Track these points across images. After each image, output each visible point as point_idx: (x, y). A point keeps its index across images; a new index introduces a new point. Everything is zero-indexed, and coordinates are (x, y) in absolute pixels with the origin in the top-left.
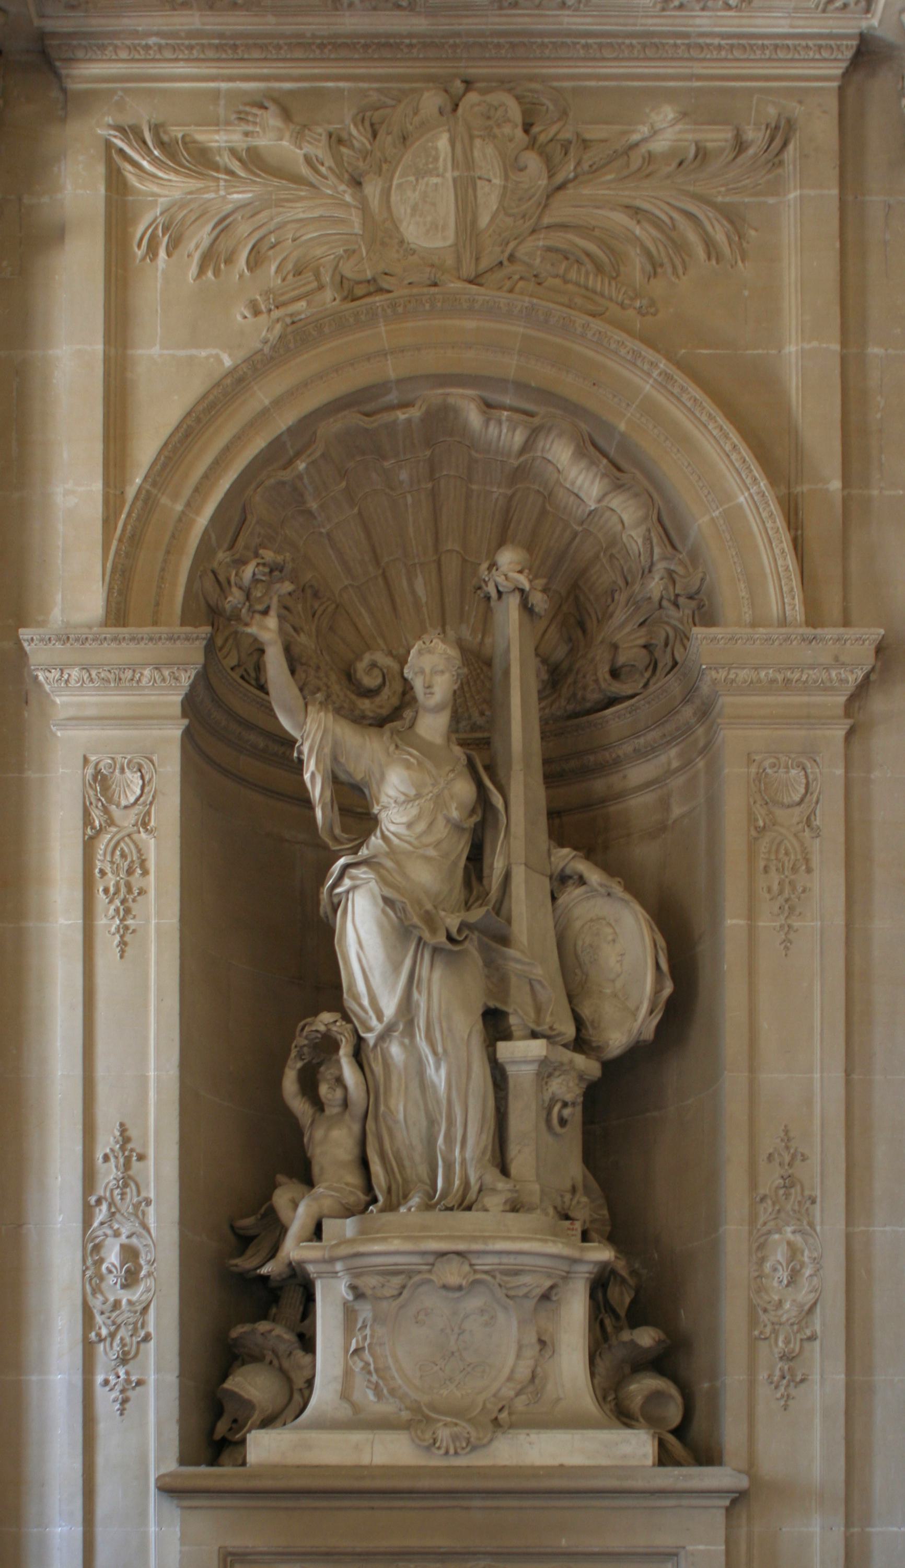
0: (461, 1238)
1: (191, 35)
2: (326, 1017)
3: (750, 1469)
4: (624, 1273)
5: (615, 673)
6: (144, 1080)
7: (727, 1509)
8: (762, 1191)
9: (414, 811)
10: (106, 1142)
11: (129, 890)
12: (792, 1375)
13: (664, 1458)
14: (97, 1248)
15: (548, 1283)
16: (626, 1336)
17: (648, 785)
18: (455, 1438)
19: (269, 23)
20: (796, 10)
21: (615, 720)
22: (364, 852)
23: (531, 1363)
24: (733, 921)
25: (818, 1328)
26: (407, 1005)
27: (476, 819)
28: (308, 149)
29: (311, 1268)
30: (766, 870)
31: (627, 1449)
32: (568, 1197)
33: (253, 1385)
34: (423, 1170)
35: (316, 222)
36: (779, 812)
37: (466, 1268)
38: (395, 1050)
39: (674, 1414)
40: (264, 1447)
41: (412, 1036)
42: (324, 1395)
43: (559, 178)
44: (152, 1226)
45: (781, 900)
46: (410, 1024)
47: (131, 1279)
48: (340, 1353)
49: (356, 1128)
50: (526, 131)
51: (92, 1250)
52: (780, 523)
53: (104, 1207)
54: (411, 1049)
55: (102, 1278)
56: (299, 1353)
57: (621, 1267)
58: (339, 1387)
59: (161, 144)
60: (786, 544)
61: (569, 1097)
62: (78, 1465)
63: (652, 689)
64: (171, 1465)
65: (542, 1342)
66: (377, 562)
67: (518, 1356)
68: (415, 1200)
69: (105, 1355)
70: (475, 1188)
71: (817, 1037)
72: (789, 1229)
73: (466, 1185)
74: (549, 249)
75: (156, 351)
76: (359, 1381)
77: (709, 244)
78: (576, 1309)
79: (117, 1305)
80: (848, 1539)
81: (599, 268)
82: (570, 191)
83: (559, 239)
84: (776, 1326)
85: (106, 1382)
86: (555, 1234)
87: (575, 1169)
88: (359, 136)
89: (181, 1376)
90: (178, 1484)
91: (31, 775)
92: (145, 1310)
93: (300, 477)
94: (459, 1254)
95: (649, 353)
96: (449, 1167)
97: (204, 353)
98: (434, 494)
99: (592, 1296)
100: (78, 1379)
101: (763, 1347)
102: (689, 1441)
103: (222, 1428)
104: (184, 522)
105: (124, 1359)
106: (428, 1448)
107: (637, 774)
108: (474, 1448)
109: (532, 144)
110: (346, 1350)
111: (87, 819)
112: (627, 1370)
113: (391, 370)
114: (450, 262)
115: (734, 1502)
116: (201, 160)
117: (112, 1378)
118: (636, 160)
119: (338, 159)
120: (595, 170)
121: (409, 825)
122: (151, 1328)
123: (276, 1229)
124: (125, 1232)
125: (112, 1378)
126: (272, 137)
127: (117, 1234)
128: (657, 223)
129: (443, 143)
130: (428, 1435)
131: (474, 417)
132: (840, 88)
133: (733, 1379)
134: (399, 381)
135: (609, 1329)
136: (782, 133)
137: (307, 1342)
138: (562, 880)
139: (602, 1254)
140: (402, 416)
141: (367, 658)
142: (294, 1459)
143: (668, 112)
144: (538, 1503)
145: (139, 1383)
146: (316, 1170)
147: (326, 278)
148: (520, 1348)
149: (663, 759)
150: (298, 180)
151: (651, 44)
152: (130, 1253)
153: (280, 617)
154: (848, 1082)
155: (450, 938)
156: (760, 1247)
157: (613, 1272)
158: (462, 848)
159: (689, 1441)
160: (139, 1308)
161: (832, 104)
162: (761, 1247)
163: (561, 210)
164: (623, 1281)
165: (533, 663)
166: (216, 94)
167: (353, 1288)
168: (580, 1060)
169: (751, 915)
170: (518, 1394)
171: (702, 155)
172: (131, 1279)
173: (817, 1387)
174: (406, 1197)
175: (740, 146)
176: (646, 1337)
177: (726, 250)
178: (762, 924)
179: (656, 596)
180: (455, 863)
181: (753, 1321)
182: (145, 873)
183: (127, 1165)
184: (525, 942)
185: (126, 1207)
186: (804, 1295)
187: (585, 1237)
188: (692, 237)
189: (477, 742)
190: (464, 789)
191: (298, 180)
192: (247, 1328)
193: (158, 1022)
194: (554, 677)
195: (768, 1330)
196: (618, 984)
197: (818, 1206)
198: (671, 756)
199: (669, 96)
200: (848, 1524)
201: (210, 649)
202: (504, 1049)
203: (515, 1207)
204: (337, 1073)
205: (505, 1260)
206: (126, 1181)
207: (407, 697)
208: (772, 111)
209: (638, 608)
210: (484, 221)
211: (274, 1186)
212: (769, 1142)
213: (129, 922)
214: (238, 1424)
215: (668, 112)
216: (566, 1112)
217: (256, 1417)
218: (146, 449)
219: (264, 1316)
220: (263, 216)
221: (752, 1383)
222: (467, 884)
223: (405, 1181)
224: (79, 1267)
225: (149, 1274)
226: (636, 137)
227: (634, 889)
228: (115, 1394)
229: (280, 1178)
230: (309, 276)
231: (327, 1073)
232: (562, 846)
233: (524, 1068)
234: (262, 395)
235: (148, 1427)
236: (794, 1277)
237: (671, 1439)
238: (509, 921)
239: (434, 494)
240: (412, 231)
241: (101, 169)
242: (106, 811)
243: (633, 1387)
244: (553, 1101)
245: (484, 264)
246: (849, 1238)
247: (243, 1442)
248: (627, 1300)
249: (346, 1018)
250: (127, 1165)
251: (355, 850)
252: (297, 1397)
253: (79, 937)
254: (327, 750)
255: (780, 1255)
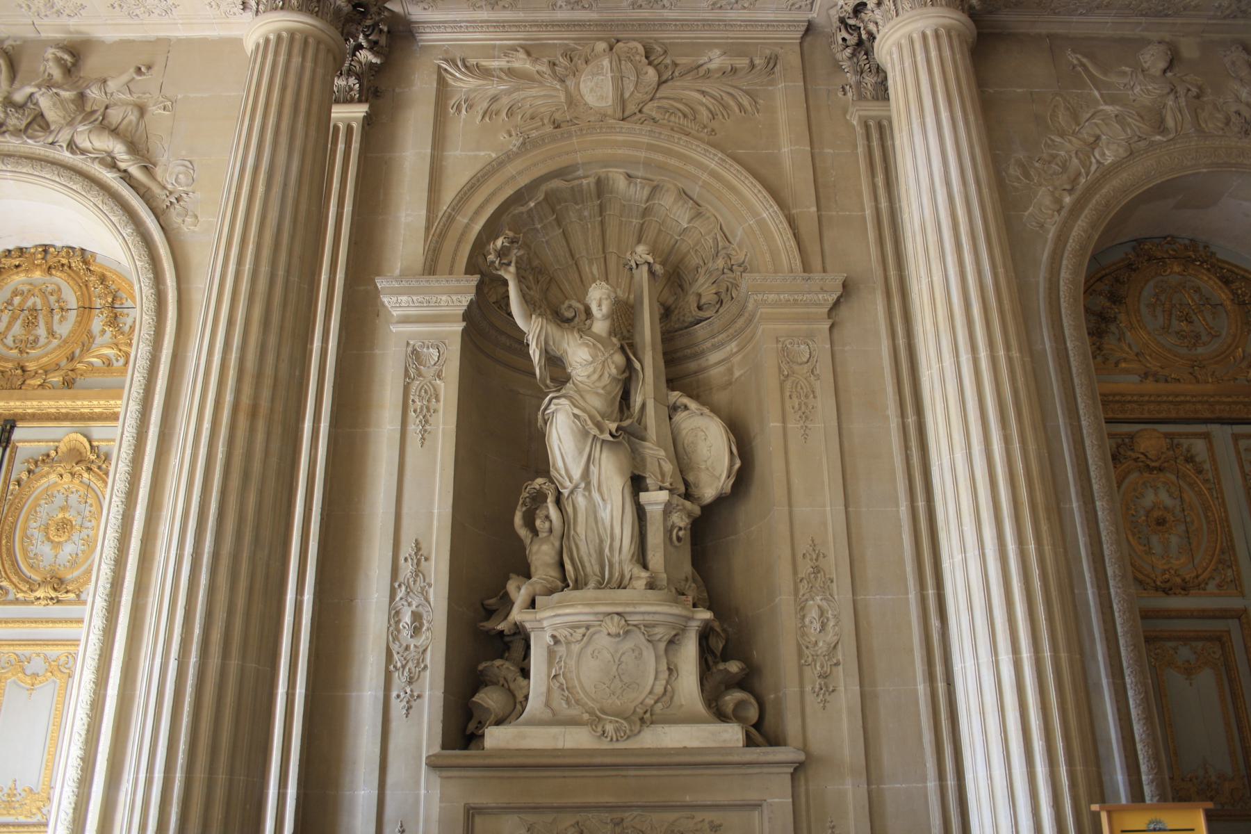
0: (620, 604)
1: (482, 21)
2: (540, 481)
3: (805, 748)
4: (718, 630)
5: (700, 308)
6: (432, 513)
7: (792, 774)
8: (800, 576)
9: (591, 369)
10: (407, 549)
11: (428, 410)
12: (827, 687)
13: (750, 742)
14: (397, 613)
15: (673, 633)
16: (721, 666)
17: (719, 362)
18: (617, 730)
19: (521, 16)
20: (777, 9)
21: (700, 331)
22: (563, 391)
23: (664, 682)
24: (774, 425)
25: (840, 658)
26: (586, 474)
27: (626, 375)
28: (538, 67)
29: (528, 625)
30: (790, 397)
31: (726, 736)
32: (683, 583)
33: (489, 699)
34: (597, 569)
35: (543, 97)
36: (796, 367)
37: (623, 622)
38: (581, 501)
39: (753, 713)
40: (495, 737)
41: (590, 492)
42: (535, 704)
43: (664, 78)
44: (432, 600)
45: (800, 413)
46: (588, 484)
47: (416, 631)
48: (545, 678)
49: (557, 544)
50: (647, 57)
51: (395, 615)
52: (786, 225)
53: (403, 588)
54: (590, 498)
55: (399, 631)
56: (520, 680)
57: (716, 625)
58: (544, 699)
59: (466, 67)
60: (790, 234)
61: (682, 525)
62: (378, 750)
63: (721, 311)
64: (437, 749)
65: (669, 669)
66: (572, 256)
67: (656, 679)
68: (592, 584)
69: (399, 680)
70: (627, 577)
71: (827, 488)
72: (818, 598)
73: (622, 576)
74: (659, 107)
75: (458, 153)
76: (556, 694)
77: (741, 106)
78: (689, 651)
79: (407, 648)
80: (869, 793)
81: (685, 116)
82: (670, 83)
83: (664, 103)
84: (815, 656)
85: (398, 696)
86: (676, 602)
87: (687, 568)
88: (563, 61)
89: (446, 692)
90: (440, 762)
91: (377, 352)
92: (425, 650)
93: (531, 210)
94: (618, 614)
95: (713, 151)
96: (611, 565)
97: (482, 153)
98: (602, 223)
99: (700, 644)
100: (381, 694)
101: (808, 672)
102: (762, 732)
103: (471, 727)
104: (467, 227)
105: (410, 682)
106: (599, 737)
107: (714, 357)
108: (629, 737)
109: (650, 64)
110: (549, 676)
111: (407, 374)
112: (723, 687)
113: (579, 158)
114: (610, 112)
115: (795, 769)
116: (486, 73)
117: (402, 695)
118: (702, 71)
119: (554, 72)
120: (681, 75)
121: (588, 377)
122: (428, 661)
123: (507, 602)
124: (414, 604)
125: (402, 695)
126: (521, 62)
127: (410, 605)
128: (713, 97)
129: (606, 62)
130: (600, 729)
131: (621, 183)
132: (801, 43)
133: (791, 691)
134: (583, 164)
135: (711, 663)
136: (772, 61)
137: (525, 673)
138: (674, 409)
139: (708, 615)
140: (585, 182)
141: (567, 303)
142: (514, 745)
143: (717, 52)
144: (671, 772)
145: (419, 697)
146: (533, 569)
147: (546, 121)
148: (657, 673)
149: (728, 348)
150: (532, 79)
151: (707, 24)
152: (417, 616)
153: (517, 268)
154: (847, 512)
155: (611, 434)
156: (802, 610)
157: (712, 629)
158: (617, 390)
159: (762, 732)
160: (421, 650)
161: (798, 49)
162: (802, 609)
163: (665, 91)
164: (718, 634)
165: (656, 305)
166: (494, 47)
167: (553, 637)
168: (688, 504)
169: (784, 421)
170: (656, 702)
171: (734, 70)
172: (416, 631)
173: (843, 695)
174: (586, 584)
175: (753, 66)
176: (734, 667)
177: (749, 108)
178: (789, 426)
179: (721, 266)
180: (614, 398)
181: (800, 654)
182: (438, 401)
183: (418, 564)
184: (655, 438)
185: (417, 588)
186: (830, 637)
187: (695, 606)
188: (732, 103)
189: (627, 343)
190: (619, 359)
191: (533, 80)
192: (488, 663)
193: (441, 482)
194: (666, 313)
195: (810, 659)
196: (709, 463)
197: (834, 585)
198: (733, 346)
199: (717, 45)
200: (868, 784)
201: (479, 288)
202: (644, 497)
203: (651, 586)
204: (544, 512)
205: (647, 617)
206: (418, 572)
207: (588, 313)
208: (768, 52)
209: (711, 274)
210: (627, 95)
211: (508, 579)
212: (803, 546)
213: (427, 427)
214: (481, 724)
215: (717, 52)
216: (681, 533)
217: (492, 718)
218: (448, 196)
219: (501, 657)
220: (515, 95)
221: (802, 693)
222: (621, 410)
223: (586, 575)
224: (386, 624)
225: (428, 629)
226: (701, 62)
227: (715, 410)
228: (404, 703)
229: (512, 575)
230: (537, 119)
231: (540, 513)
232: (673, 390)
233: (655, 507)
234: (510, 169)
235: (422, 726)
236: (823, 626)
237: (753, 730)
238: (646, 429)
239: (602, 223)
240: (590, 99)
241: (435, 77)
242: (417, 369)
243: (728, 698)
244: (673, 526)
245: (627, 114)
246: (855, 602)
247: (483, 736)
248: (721, 646)
249: (553, 483)
250: (418, 564)
251: (559, 391)
252: (518, 706)
253: (398, 436)
254: (543, 338)
255: (814, 613)
